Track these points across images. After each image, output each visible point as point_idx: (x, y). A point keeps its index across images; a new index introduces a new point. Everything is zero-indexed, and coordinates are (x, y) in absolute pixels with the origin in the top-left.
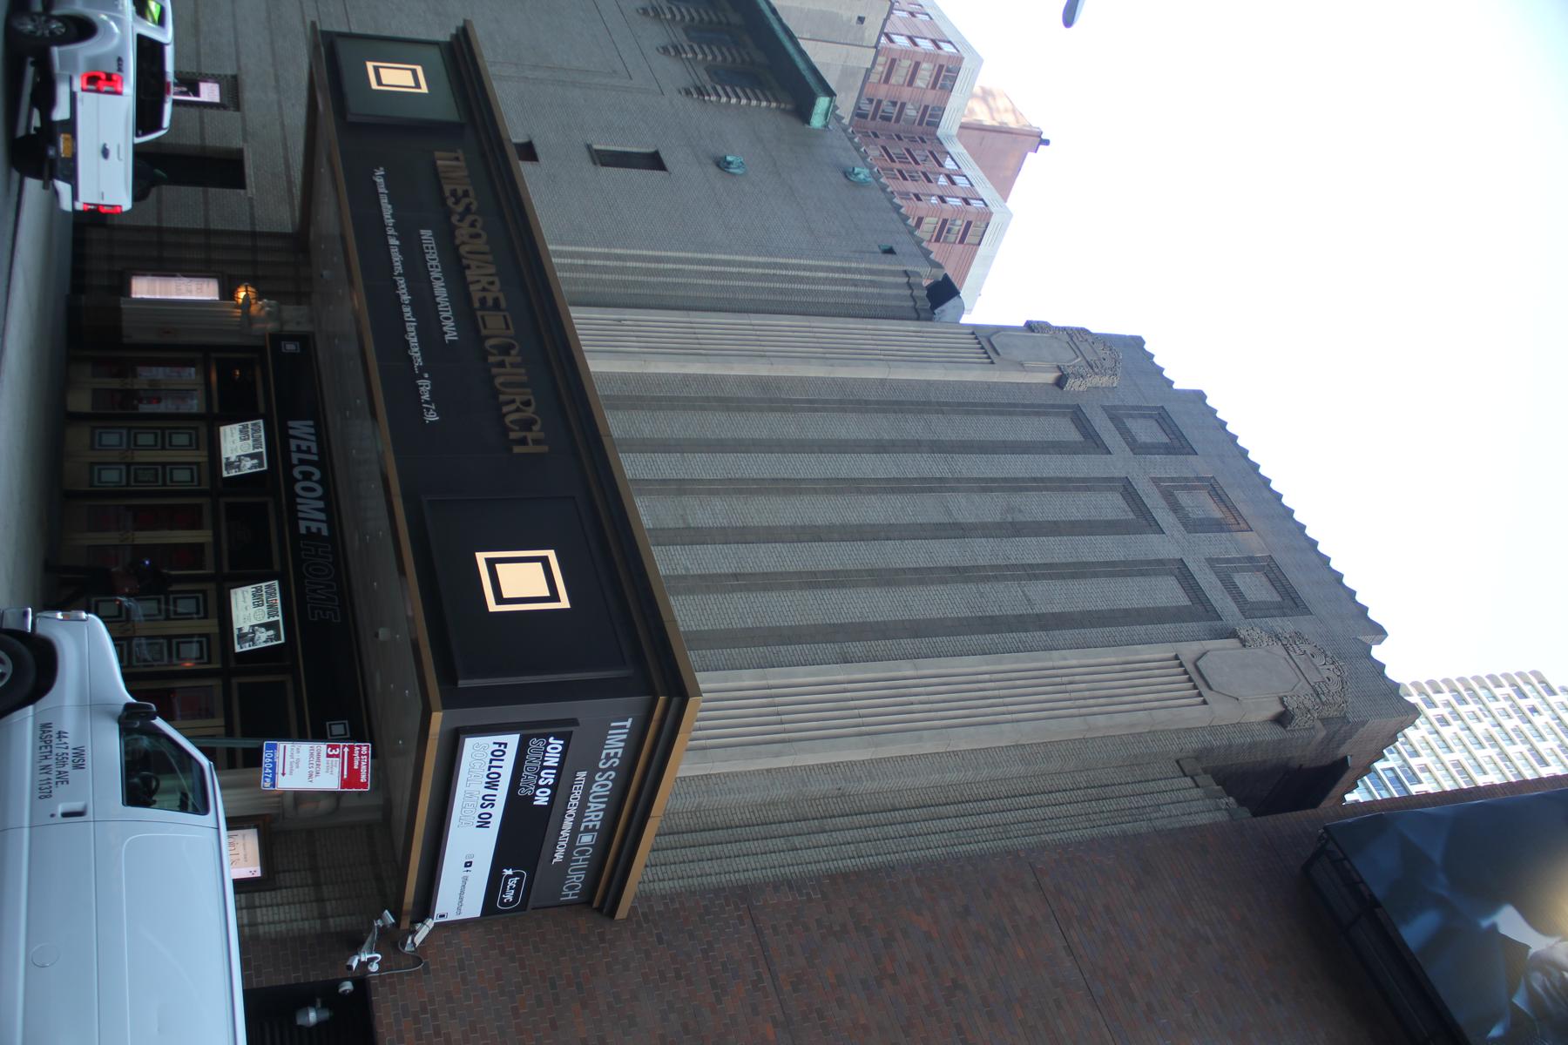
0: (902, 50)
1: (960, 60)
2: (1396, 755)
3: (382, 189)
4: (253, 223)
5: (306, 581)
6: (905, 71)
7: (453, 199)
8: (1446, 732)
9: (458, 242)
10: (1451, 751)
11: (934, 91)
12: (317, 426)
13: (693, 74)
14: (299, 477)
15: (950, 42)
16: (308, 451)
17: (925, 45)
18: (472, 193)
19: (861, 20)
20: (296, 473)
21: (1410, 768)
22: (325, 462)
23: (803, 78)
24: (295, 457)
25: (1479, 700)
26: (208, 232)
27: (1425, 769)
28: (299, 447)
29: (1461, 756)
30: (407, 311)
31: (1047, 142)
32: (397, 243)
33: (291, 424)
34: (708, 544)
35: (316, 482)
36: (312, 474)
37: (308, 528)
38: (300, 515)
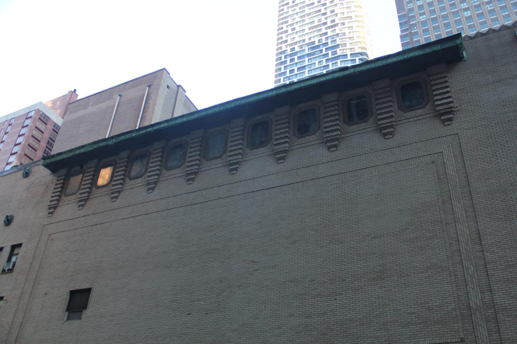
0: (29, 131)
1: (38, 111)
2: (303, 46)
6: (37, 133)
8: (297, 29)
10: (305, 29)
11: (48, 125)
13: (419, 118)
15: (29, 113)
17: (27, 122)
19: (168, 87)
21: (309, 43)
23: (434, 52)
25: (287, 17)
27: (310, 39)
29: (307, 28)
31: (75, 90)
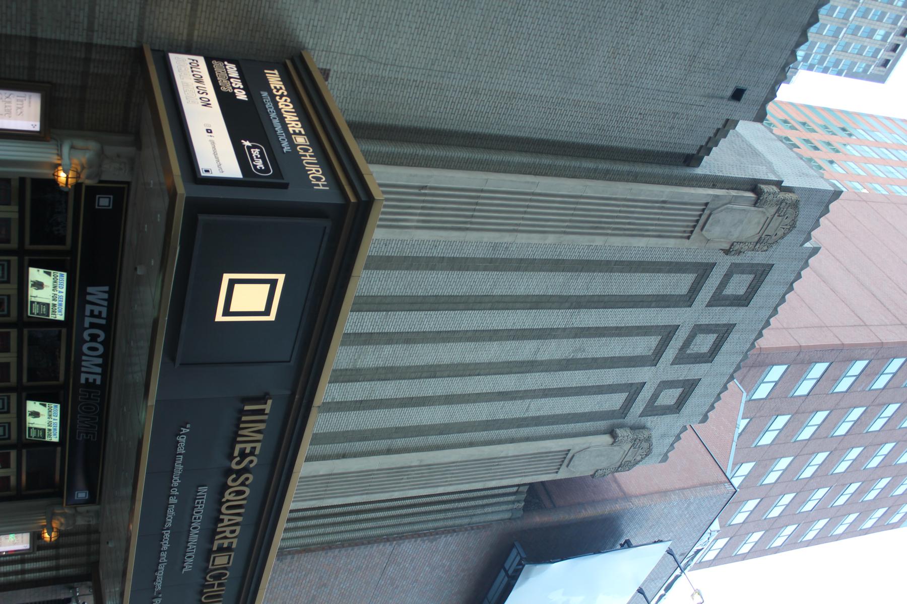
3: (181, 450)
4: (91, 29)
5: (79, 415)
7: (238, 459)
9: (224, 500)
12: (111, 293)
14: (87, 338)
16: (99, 316)
18: (257, 452)
20: (86, 336)
22: (109, 328)
24: (87, 321)
26: (34, 40)
28: (92, 311)
30: (164, 555)
32: (176, 501)
33: (90, 289)
34: (359, 381)
35: (100, 343)
36: (98, 336)
37: (87, 379)
38: (83, 369)
